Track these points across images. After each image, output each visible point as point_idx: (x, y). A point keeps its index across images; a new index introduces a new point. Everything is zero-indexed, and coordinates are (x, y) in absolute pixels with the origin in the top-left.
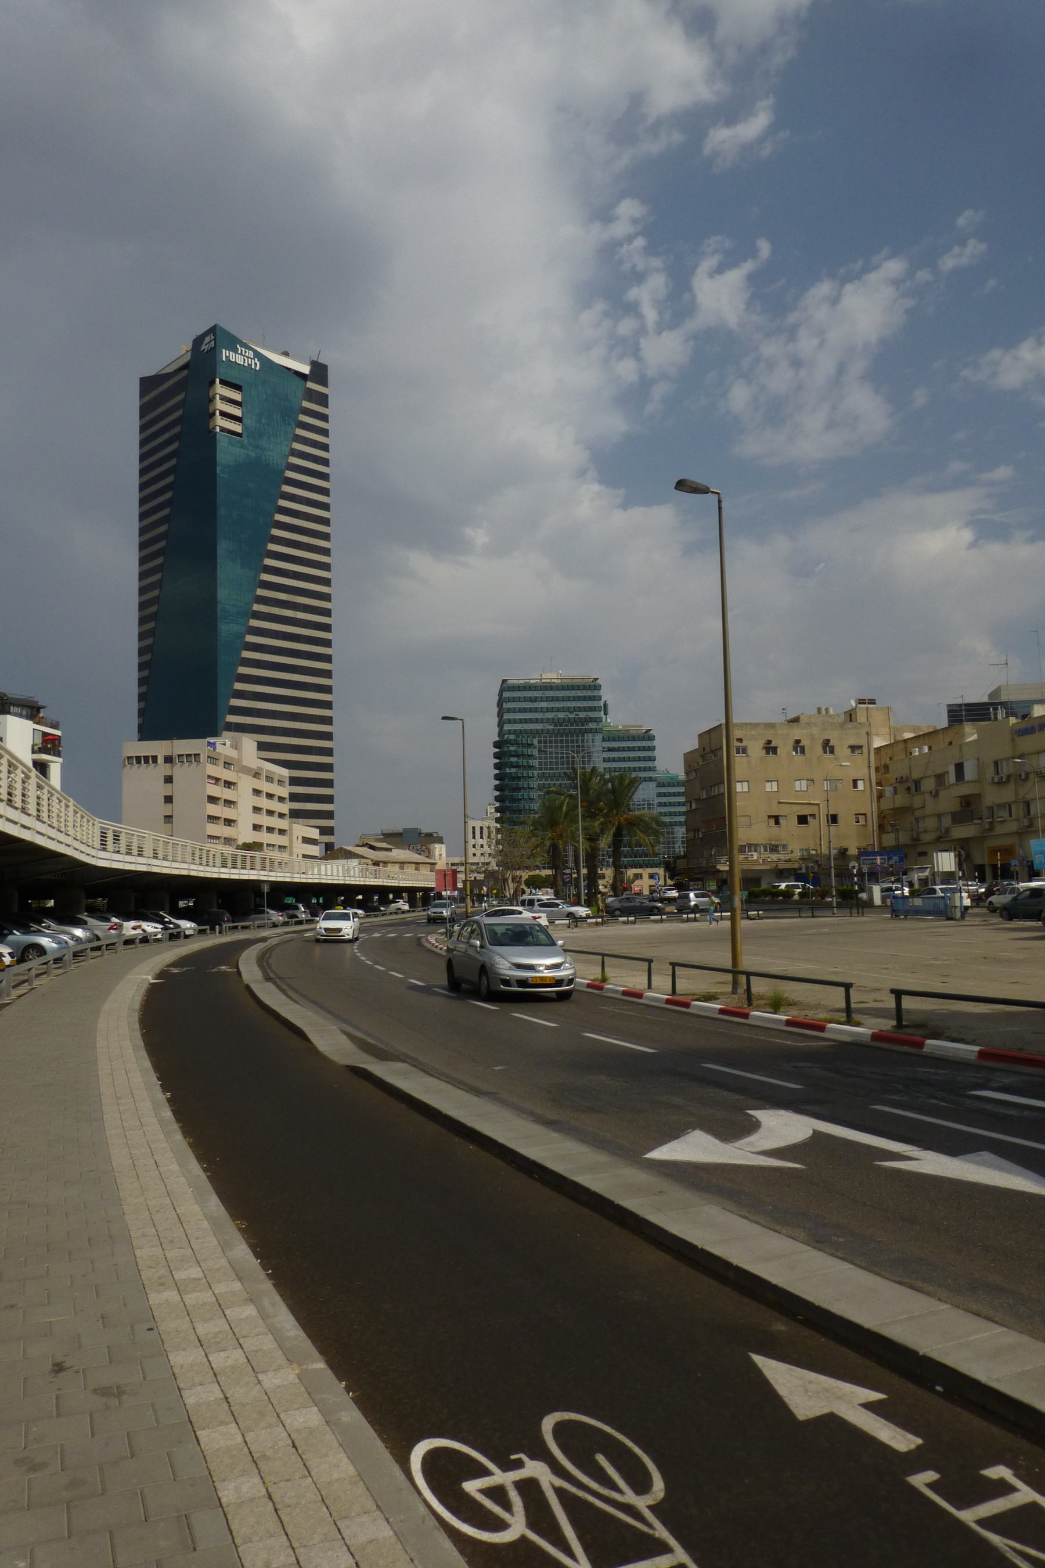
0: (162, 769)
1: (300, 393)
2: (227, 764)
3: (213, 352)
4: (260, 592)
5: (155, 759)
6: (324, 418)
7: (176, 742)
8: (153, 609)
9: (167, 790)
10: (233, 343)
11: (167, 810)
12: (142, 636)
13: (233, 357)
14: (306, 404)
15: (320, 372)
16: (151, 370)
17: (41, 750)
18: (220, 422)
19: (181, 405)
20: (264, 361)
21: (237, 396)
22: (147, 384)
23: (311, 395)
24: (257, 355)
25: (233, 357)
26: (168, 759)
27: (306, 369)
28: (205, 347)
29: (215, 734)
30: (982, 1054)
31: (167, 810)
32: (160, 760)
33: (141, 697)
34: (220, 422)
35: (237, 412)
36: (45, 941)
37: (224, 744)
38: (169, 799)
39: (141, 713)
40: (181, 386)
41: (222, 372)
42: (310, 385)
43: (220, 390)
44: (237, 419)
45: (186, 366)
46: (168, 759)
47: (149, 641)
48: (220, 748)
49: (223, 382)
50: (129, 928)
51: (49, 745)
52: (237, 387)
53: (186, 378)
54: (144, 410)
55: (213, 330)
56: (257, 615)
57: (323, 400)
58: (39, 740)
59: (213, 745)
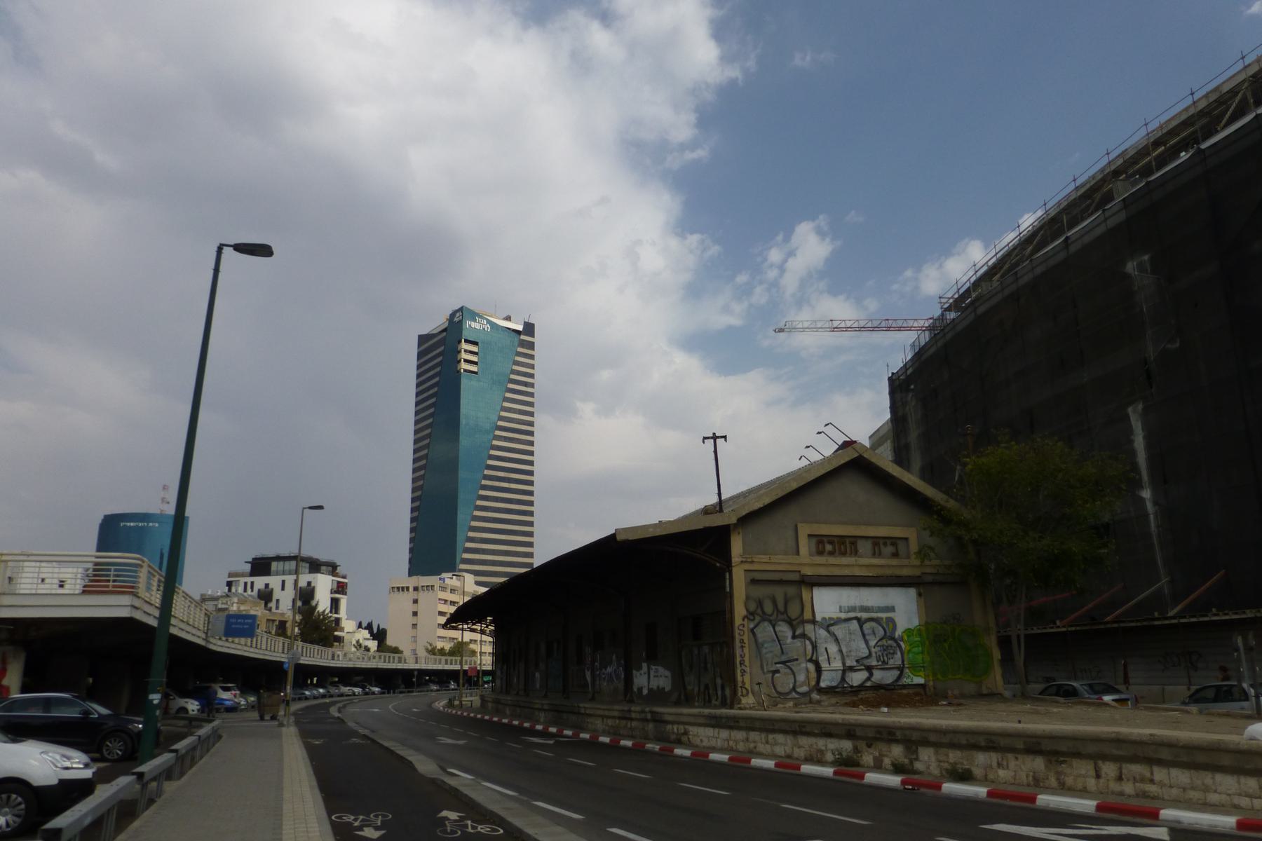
0: (411, 595)
1: (516, 343)
2: (453, 591)
3: (460, 322)
4: (486, 472)
5: (408, 588)
6: (532, 357)
7: (421, 578)
8: (421, 483)
9: (414, 607)
10: (474, 315)
11: (414, 620)
12: (413, 500)
13: (473, 325)
14: (520, 350)
15: (529, 328)
17: (337, 592)
18: (464, 366)
20: (493, 325)
21: (475, 349)
22: (423, 339)
23: (524, 344)
24: (489, 322)
25: (473, 325)
26: (416, 589)
27: (520, 328)
28: (456, 319)
29: (451, 567)
30: (1099, 808)
31: (414, 620)
32: (411, 589)
33: (412, 540)
34: (464, 366)
35: (475, 358)
37: (450, 580)
38: (415, 614)
39: (411, 550)
40: (442, 342)
41: (466, 334)
42: (523, 337)
43: (464, 346)
44: (475, 363)
46: (416, 589)
47: (417, 504)
48: (447, 581)
49: (466, 341)
50: (345, 689)
51: (341, 588)
52: (475, 343)
53: (444, 338)
54: (420, 355)
55: (461, 309)
56: (485, 488)
57: (531, 346)
58: (335, 586)
59: (443, 580)
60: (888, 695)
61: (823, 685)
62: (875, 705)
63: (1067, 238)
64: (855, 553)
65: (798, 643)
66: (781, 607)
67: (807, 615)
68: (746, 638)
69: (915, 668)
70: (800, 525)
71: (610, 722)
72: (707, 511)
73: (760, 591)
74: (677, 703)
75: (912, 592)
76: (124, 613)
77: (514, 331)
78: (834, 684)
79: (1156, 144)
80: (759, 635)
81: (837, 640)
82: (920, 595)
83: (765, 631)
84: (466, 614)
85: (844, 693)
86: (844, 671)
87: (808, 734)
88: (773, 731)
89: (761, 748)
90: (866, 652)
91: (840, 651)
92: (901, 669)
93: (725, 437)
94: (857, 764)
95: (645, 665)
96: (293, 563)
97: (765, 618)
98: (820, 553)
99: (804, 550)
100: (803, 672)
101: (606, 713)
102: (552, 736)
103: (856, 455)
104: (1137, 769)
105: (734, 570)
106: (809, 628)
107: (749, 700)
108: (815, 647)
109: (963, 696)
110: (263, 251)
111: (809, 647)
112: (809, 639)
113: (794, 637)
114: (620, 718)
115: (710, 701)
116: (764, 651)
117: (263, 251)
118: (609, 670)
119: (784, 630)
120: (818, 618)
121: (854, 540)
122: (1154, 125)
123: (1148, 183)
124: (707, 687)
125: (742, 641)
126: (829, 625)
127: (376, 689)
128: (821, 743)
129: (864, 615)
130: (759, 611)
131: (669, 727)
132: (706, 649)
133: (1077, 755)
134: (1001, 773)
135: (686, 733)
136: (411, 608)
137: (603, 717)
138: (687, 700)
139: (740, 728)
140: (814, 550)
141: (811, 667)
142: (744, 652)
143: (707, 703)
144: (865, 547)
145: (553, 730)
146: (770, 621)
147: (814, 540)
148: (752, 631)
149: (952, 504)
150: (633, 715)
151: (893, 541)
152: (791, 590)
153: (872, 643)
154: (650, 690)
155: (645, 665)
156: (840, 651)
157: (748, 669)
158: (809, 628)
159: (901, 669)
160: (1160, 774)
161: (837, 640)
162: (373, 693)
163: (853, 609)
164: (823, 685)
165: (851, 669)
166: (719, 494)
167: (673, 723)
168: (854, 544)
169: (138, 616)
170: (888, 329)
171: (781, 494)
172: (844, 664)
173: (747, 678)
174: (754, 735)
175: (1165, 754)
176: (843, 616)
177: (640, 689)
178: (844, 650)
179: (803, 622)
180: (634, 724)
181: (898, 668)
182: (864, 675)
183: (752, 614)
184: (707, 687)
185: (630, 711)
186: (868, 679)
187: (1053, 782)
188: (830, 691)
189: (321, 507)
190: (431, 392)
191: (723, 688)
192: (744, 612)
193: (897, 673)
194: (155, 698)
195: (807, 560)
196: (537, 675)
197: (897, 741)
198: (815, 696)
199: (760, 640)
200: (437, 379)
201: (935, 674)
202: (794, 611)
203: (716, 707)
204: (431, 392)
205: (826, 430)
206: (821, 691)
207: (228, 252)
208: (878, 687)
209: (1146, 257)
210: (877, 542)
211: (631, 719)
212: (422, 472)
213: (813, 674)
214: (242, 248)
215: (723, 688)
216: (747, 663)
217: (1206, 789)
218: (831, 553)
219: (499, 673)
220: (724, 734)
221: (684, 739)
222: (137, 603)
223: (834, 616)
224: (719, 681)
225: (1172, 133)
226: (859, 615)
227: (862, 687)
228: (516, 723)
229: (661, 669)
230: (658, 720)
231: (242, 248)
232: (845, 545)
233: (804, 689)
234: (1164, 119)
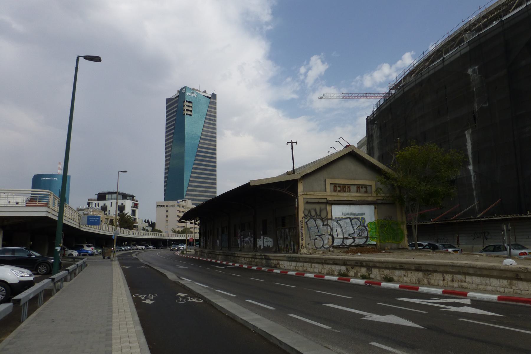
0: (165, 209)
2: (183, 207)
3: (185, 93)
5: (164, 206)
8: (168, 162)
12: (165, 169)
15: (214, 96)
16: (169, 97)
17: (134, 207)
19: (177, 107)
22: (168, 100)
27: (210, 96)
28: (183, 92)
29: (182, 198)
33: (165, 186)
34: (186, 112)
35: (190, 109)
36: (123, 248)
37: (182, 203)
38: (167, 216)
39: (165, 190)
40: (177, 102)
43: (186, 103)
45: (178, 97)
46: (167, 206)
47: (167, 171)
51: (136, 206)
52: (191, 102)
54: (167, 107)
55: (185, 87)
57: (215, 103)
58: (133, 205)
60: (361, 249)
61: (335, 244)
62: (355, 252)
63: (444, 58)
64: (349, 191)
65: (325, 228)
66: (318, 213)
67: (329, 216)
68: (303, 226)
69: (372, 238)
70: (327, 180)
71: (247, 259)
72: (288, 173)
73: (310, 207)
74: (275, 252)
75: (372, 207)
76: (44, 214)
77: (208, 97)
78: (339, 244)
79: (484, 17)
80: (309, 225)
81: (341, 226)
82: (375, 208)
83: (311, 223)
84: (188, 216)
85: (343, 248)
86: (343, 239)
87: (328, 264)
88: (314, 263)
89: (309, 269)
90: (353, 232)
91: (342, 231)
92: (367, 238)
93: (296, 142)
94: (348, 276)
95: (262, 237)
96: (115, 195)
97: (311, 217)
98: (335, 191)
99: (328, 189)
100: (327, 239)
101: (246, 256)
102: (223, 265)
103: (351, 150)
104: (459, 277)
105: (299, 198)
106: (329, 222)
107: (304, 251)
108: (332, 229)
109: (391, 249)
110: (97, 59)
111: (330, 229)
112: (330, 226)
113: (323, 225)
114: (252, 258)
115: (288, 251)
116: (311, 231)
117: (97, 59)
118: (247, 239)
119: (319, 222)
120: (334, 218)
121: (349, 186)
122: (483, 9)
123: (479, 35)
124: (287, 245)
125: (302, 227)
126: (338, 220)
127: (152, 247)
128: (333, 267)
129: (352, 217)
130: (309, 215)
131: (272, 261)
132: (287, 230)
133: (436, 271)
134: (405, 278)
135: (278, 264)
136: (165, 214)
137: (245, 257)
138: (279, 251)
139: (300, 262)
140: (332, 189)
141: (330, 237)
142: (303, 231)
143: (287, 252)
144: (353, 189)
145: (224, 263)
146: (314, 219)
147: (333, 186)
148: (306, 223)
149: (390, 171)
150: (257, 257)
151: (365, 186)
152: (323, 206)
153: (355, 228)
154: (264, 247)
155: (262, 237)
156: (342, 231)
157: (304, 238)
158: (329, 222)
159: (367, 238)
160: (468, 279)
161: (341, 226)
162: (150, 248)
163: (348, 214)
164: (335, 244)
165: (346, 238)
166: (294, 166)
167: (273, 260)
168: (349, 187)
169: (50, 216)
170: (367, 97)
171: (319, 166)
172: (343, 236)
173: (304, 242)
174: (306, 264)
175: (471, 271)
176: (344, 217)
177: (260, 247)
178: (344, 231)
179: (327, 219)
180: (257, 260)
181: (365, 238)
182: (352, 240)
183: (306, 216)
184: (287, 245)
185: (256, 255)
186: (353, 242)
187: (426, 282)
188: (338, 247)
189: (126, 172)
190: (172, 123)
191: (294, 246)
192: (303, 215)
193: (365, 240)
194: (58, 249)
195: (330, 194)
196: (218, 241)
197: (364, 266)
198: (332, 249)
199: (309, 227)
200: (175, 118)
201: (380, 240)
202: (323, 215)
203: (291, 253)
204: (172, 123)
205: (340, 140)
206: (334, 247)
207: (81, 60)
208: (357, 245)
209: (477, 67)
210: (359, 187)
211: (257, 258)
212: (169, 158)
213: (331, 241)
214: (87, 58)
215: (294, 246)
216: (304, 235)
217: (487, 285)
218: (340, 191)
219: (202, 240)
220: (294, 264)
221: (278, 266)
222: (49, 210)
223: (340, 217)
224: (292, 243)
225: (491, 13)
226: (350, 216)
227: (350, 245)
228: (209, 260)
229: (269, 239)
230: (267, 258)
231: (87, 58)
232: (345, 188)
233: (327, 246)
234: (487, 6)
